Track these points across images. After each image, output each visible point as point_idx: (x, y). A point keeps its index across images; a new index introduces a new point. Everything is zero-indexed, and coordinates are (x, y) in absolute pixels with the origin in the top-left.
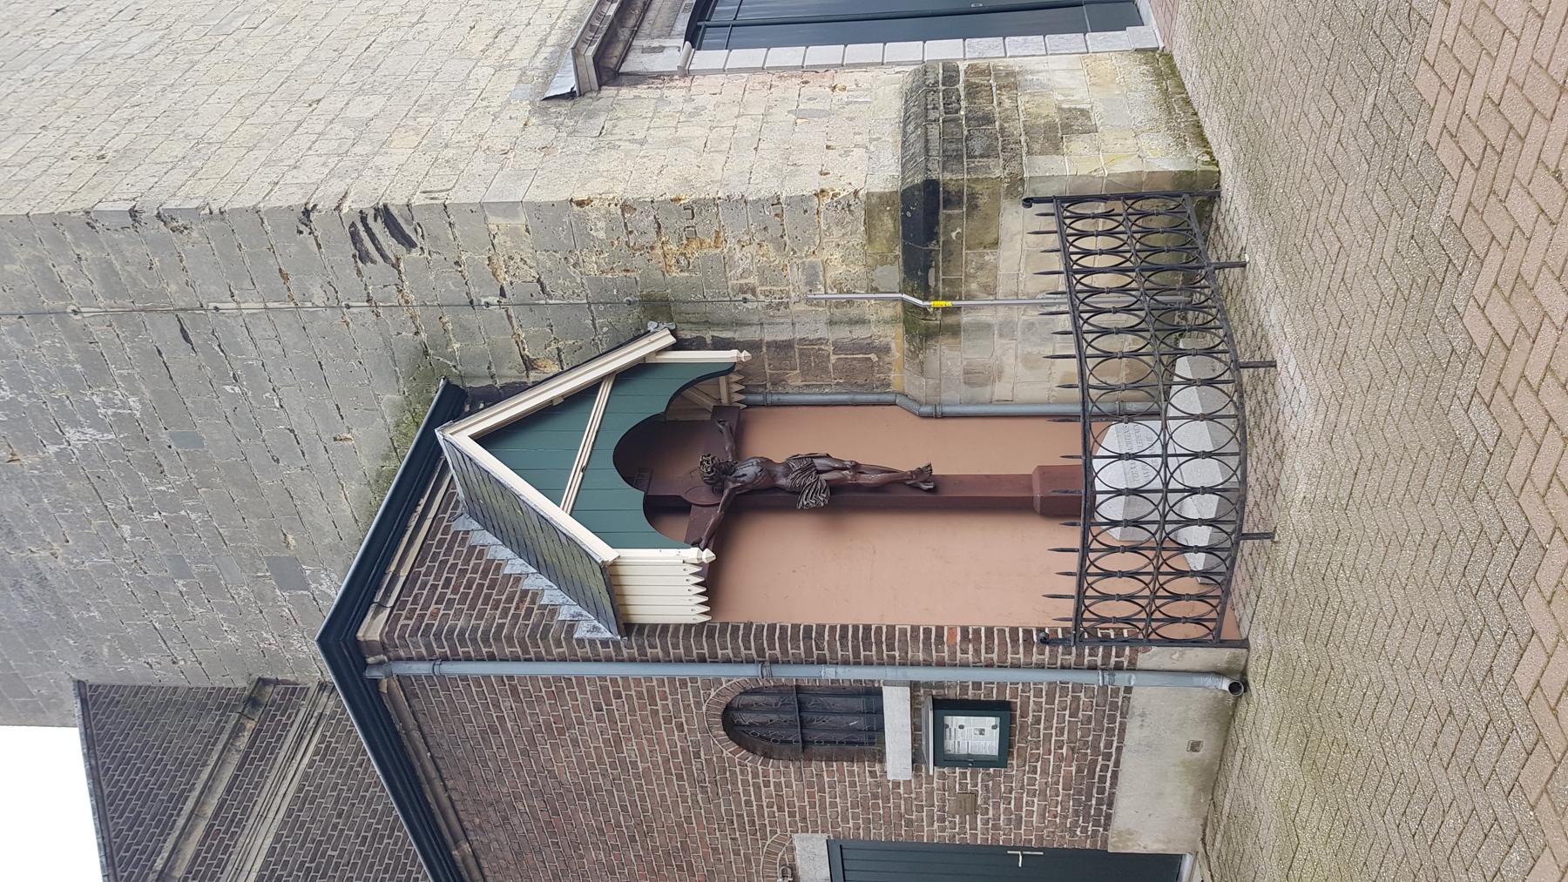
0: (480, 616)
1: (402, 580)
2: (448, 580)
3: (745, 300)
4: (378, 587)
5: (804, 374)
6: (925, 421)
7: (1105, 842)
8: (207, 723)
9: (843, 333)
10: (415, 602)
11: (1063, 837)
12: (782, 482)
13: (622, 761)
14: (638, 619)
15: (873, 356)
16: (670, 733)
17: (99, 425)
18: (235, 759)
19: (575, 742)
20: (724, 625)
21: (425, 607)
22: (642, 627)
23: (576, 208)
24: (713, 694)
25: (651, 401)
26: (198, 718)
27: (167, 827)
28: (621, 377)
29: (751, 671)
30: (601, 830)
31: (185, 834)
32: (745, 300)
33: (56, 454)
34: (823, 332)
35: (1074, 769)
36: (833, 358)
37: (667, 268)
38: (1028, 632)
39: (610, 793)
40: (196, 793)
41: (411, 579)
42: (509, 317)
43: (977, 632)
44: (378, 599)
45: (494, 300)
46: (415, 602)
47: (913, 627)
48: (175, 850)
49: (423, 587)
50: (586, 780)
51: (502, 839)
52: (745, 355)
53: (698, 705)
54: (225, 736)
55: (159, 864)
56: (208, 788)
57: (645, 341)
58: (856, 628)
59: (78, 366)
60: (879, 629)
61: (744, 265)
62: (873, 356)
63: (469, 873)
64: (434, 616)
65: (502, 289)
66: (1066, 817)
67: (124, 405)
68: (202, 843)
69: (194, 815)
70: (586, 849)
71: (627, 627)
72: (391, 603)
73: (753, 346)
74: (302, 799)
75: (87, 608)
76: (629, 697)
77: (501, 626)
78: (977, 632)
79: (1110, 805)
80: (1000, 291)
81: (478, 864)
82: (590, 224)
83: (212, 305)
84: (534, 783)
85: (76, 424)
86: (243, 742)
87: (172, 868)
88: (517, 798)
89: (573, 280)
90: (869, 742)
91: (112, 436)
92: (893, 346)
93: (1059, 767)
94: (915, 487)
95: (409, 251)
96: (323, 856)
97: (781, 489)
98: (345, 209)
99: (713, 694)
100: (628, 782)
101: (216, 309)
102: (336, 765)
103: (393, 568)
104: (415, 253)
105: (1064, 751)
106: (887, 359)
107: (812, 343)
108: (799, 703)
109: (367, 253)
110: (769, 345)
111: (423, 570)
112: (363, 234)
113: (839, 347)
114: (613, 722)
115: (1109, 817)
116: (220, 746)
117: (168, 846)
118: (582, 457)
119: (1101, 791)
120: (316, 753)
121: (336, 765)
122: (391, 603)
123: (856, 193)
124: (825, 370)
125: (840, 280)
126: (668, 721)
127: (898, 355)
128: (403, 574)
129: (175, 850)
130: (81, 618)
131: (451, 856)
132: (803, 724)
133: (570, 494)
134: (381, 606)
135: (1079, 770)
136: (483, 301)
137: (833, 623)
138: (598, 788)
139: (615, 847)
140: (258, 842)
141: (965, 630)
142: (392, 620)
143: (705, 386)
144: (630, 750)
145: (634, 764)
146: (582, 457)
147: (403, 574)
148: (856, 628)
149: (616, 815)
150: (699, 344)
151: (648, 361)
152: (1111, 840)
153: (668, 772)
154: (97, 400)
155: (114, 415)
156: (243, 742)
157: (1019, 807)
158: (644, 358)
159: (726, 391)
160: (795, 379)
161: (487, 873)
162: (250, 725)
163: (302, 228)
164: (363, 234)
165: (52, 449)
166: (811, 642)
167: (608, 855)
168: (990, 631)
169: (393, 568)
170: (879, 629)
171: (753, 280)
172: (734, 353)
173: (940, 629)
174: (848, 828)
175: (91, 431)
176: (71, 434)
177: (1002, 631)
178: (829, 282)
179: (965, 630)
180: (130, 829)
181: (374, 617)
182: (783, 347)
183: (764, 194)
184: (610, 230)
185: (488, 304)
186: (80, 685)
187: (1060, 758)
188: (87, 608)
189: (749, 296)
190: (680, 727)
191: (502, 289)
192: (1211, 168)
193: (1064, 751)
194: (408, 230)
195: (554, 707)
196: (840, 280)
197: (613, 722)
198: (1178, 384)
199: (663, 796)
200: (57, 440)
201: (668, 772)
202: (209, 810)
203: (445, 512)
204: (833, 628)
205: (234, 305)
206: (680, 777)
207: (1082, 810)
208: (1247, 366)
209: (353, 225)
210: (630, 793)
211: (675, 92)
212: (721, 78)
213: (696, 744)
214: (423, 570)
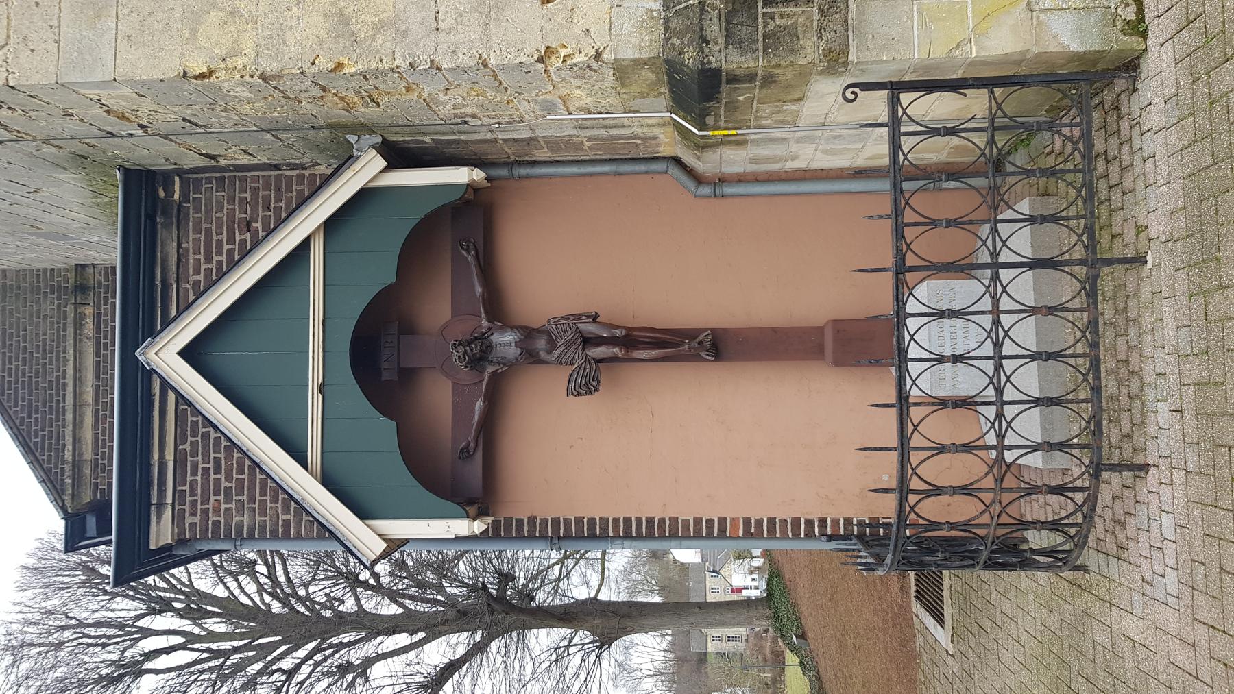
0: (263, 512)
1: (171, 465)
2: (217, 461)
4: (149, 484)
8: (48, 308)
10: (193, 493)
18: (89, 346)
20: (508, 520)
21: (206, 501)
26: (38, 302)
28: (331, 225)
31: (77, 424)
38: (810, 523)
40: (70, 388)
41: (180, 461)
43: (759, 523)
44: (154, 500)
46: (193, 493)
48: (76, 440)
49: (195, 473)
52: (478, 175)
54: (70, 330)
55: (68, 456)
56: (78, 381)
57: (348, 174)
58: (639, 520)
60: (662, 521)
64: (217, 511)
68: (96, 427)
69: (78, 406)
72: (169, 500)
77: (287, 524)
78: (759, 523)
80: (801, 123)
86: (89, 328)
87: (81, 455)
103: (156, 456)
111: (187, 446)
116: (70, 341)
117: (69, 439)
118: (315, 374)
122: (169, 500)
123: (598, 56)
128: (170, 456)
129: (76, 440)
133: (314, 453)
134: (161, 505)
141: (747, 521)
142: (178, 518)
146: (315, 374)
147: (170, 456)
148: (639, 520)
156: (89, 328)
162: (89, 311)
168: (772, 521)
169: (156, 456)
170: (662, 521)
173: (722, 520)
177: (784, 522)
179: (747, 521)
181: (158, 522)
183: (463, 60)
192: (1134, 42)
198: (1013, 174)
202: (89, 398)
204: (616, 521)
208: (1112, 468)
214: (187, 446)
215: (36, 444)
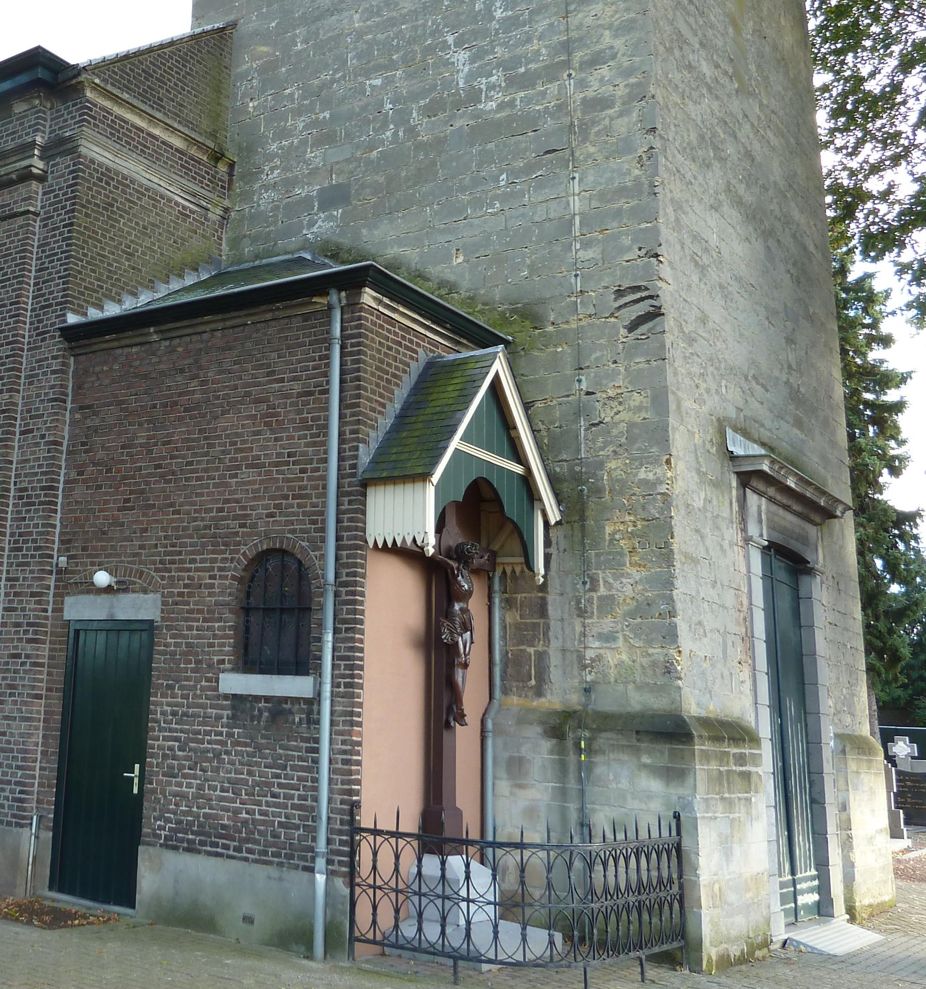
3: (584, 583)
5: (518, 627)
6: (479, 723)
7: (148, 844)
9: (554, 659)
11: (155, 810)
12: (457, 607)
13: (239, 467)
14: (371, 492)
15: (533, 682)
16: (266, 507)
17: (471, 77)
19: (258, 433)
22: (365, 495)
23: (665, 458)
24: (303, 544)
25: (512, 506)
27: (143, 97)
29: (331, 576)
30: (169, 443)
32: (584, 583)
33: (446, 41)
34: (555, 644)
35: (226, 822)
36: (531, 650)
37: (616, 527)
39: (207, 454)
42: (568, 396)
45: (584, 386)
47: (362, 703)
50: (220, 437)
51: (162, 366)
53: (293, 531)
59: (522, 70)
61: (617, 585)
62: (533, 682)
63: (128, 338)
65: (593, 393)
66: (175, 813)
67: (489, 98)
70: (148, 430)
71: (365, 484)
73: (544, 588)
74: (156, 198)
75: (306, 41)
76: (302, 479)
79: (188, 850)
81: (136, 345)
82: (651, 467)
83: (577, 175)
84: (218, 398)
85: (472, 60)
88: (203, 383)
89: (603, 449)
90: (249, 662)
91: (461, 85)
92: (543, 700)
93: (227, 810)
94: (449, 710)
95: (625, 327)
96: (121, 216)
97: (450, 604)
98: (660, 284)
99: (303, 544)
100: (217, 469)
101: (574, 178)
102: (175, 222)
104: (623, 332)
105: (244, 815)
106: (530, 694)
107: (546, 634)
108: (293, 609)
109: (622, 296)
110: (544, 599)
112: (638, 295)
113: (541, 657)
114: (277, 464)
115: (175, 848)
119: (202, 843)
120: (184, 207)
121: (175, 222)
124: (521, 642)
125: (603, 656)
126: (276, 506)
127: (535, 703)
130: (296, 36)
131: (149, 326)
132: (267, 611)
135: (224, 827)
136: (583, 378)
137: (366, 642)
138: (210, 446)
139: (150, 452)
140: (133, 167)
143: (518, 548)
144: (248, 475)
145: (236, 476)
149: (183, 457)
150: (548, 543)
151: (536, 504)
152: (151, 849)
153: (227, 501)
154: (494, 79)
155: (481, 90)
157: (185, 776)
158: (540, 500)
159: (511, 561)
160: (512, 617)
161: (126, 350)
163: (644, 251)
164: (638, 295)
165: (450, 39)
166: (349, 625)
167: (141, 445)
171: (602, 591)
172: (542, 572)
174: (167, 641)
175: (466, 69)
176: (462, 56)
178: (602, 651)
180: (143, 71)
182: (542, 610)
184: (645, 482)
185: (579, 381)
186: (234, 25)
187: (236, 812)
188: (306, 41)
189: (588, 586)
190: (271, 515)
191: (593, 393)
193: (244, 815)
194: (643, 328)
195: (293, 421)
196: (603, 656)
197: (277, 464)
199: (202, 495)
200: (459, 43)
201: (227, 501)
203: (400, 328)
205: (577, 191)
206: (221, 510)
207: (182, 827)
209: (647, 289)
210: (206, 470)
211: (732, 534)
212: (743, 570)
213: (254, 526)
215: (125, 66)
